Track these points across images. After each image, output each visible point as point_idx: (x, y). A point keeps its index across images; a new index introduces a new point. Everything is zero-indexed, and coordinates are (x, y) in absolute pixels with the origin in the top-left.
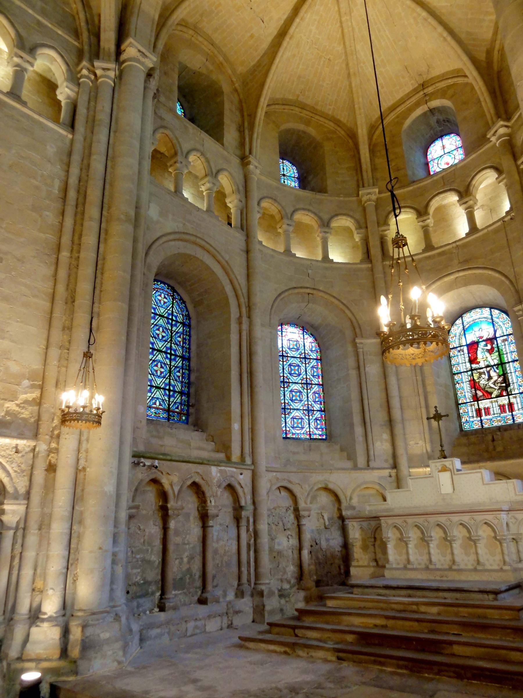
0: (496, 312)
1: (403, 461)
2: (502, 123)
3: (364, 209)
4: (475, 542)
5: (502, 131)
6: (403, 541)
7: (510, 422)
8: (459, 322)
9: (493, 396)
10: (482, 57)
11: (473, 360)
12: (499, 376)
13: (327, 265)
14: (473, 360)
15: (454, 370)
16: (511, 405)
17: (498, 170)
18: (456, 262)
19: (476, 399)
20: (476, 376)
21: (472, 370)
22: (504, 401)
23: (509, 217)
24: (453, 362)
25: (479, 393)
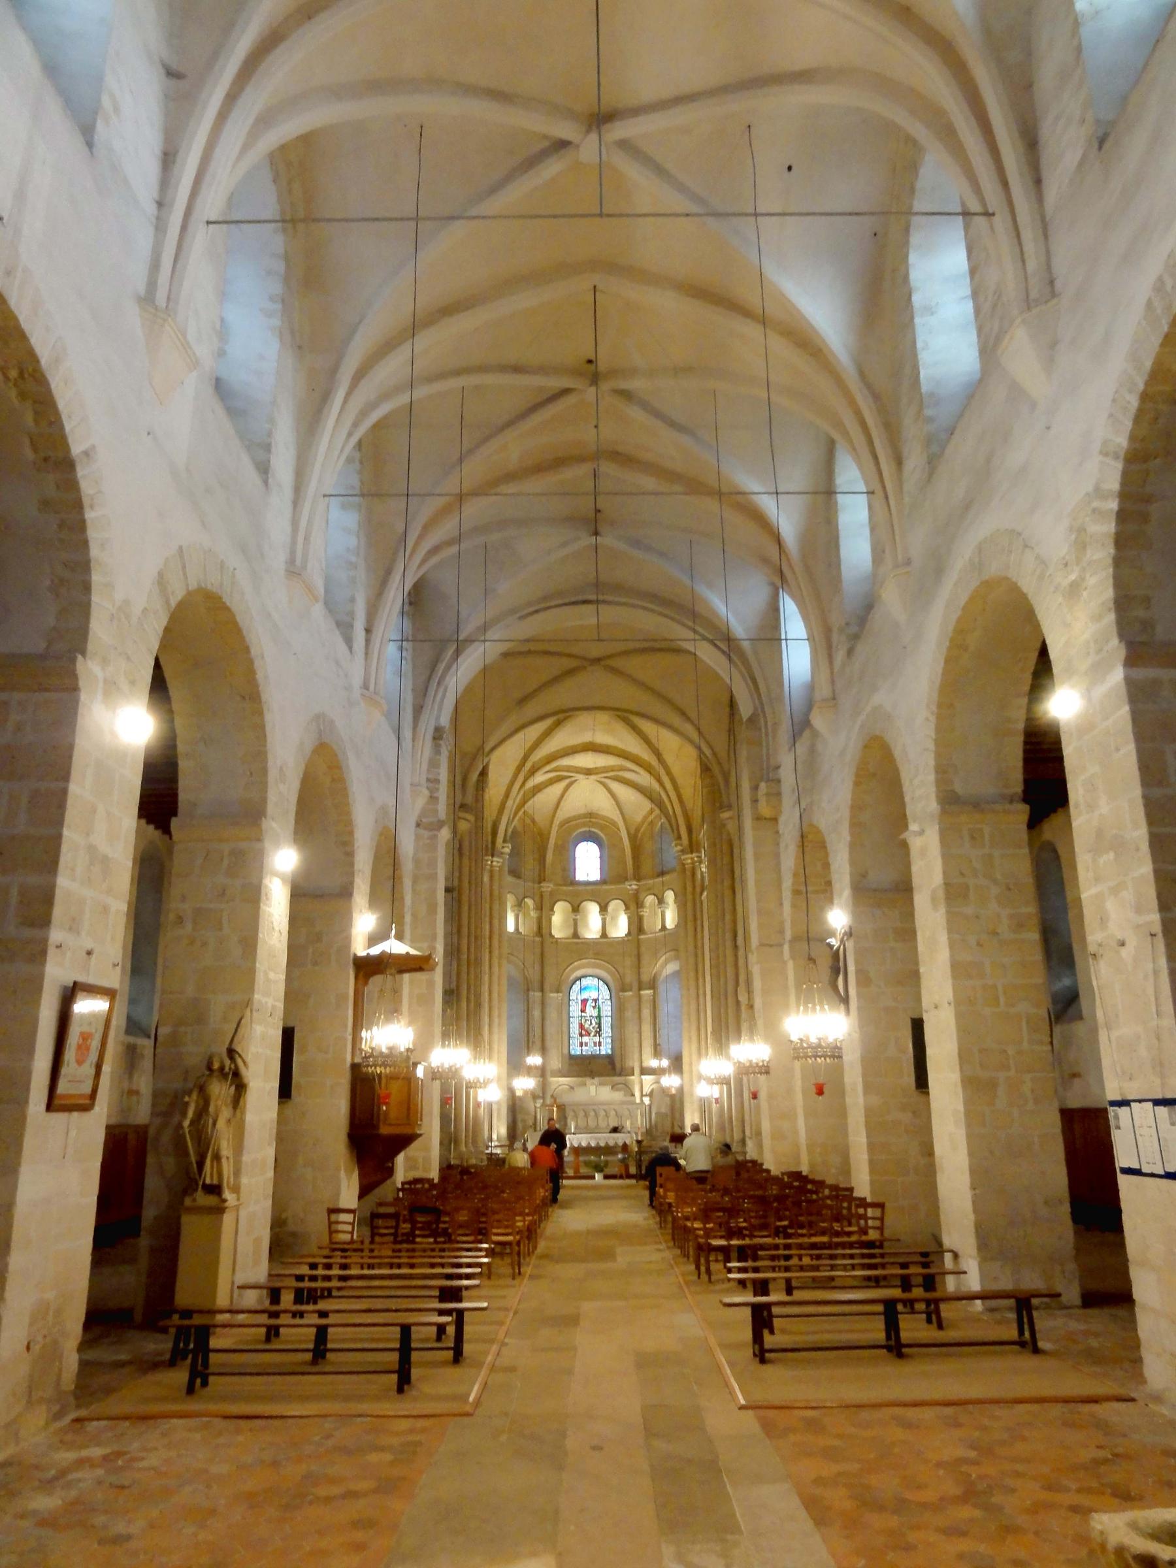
0: (601, 983)
1: (548, 1073)
2: (635, 883)
3: (542, 896)
4: (608, 1117)
5: (634, 887)
6: (576, 1117)
7: (598, 1053)
8: (578, 982)
9: (592, 1035)
10: (632, 831)
11: (583, 1011)
12: (596, 1023)
13: (518, 936)
14: (583, 1011)
15: (571, 1015)
16: (600, 1043)
17: (627, 908)
18: (591, 952)
19: (581, 1035)
20: (583, 1021)
21: (581, 1016)
22: (597, 1039)
23: (626, 939)
24: (571, 1009)
25: (584, 1032)
